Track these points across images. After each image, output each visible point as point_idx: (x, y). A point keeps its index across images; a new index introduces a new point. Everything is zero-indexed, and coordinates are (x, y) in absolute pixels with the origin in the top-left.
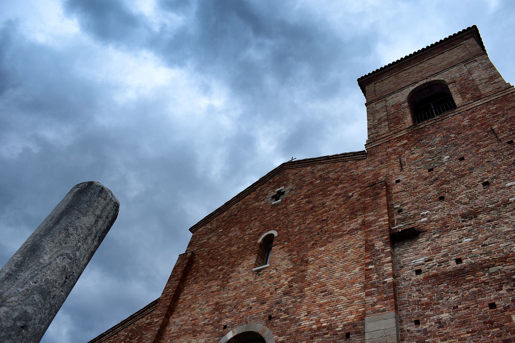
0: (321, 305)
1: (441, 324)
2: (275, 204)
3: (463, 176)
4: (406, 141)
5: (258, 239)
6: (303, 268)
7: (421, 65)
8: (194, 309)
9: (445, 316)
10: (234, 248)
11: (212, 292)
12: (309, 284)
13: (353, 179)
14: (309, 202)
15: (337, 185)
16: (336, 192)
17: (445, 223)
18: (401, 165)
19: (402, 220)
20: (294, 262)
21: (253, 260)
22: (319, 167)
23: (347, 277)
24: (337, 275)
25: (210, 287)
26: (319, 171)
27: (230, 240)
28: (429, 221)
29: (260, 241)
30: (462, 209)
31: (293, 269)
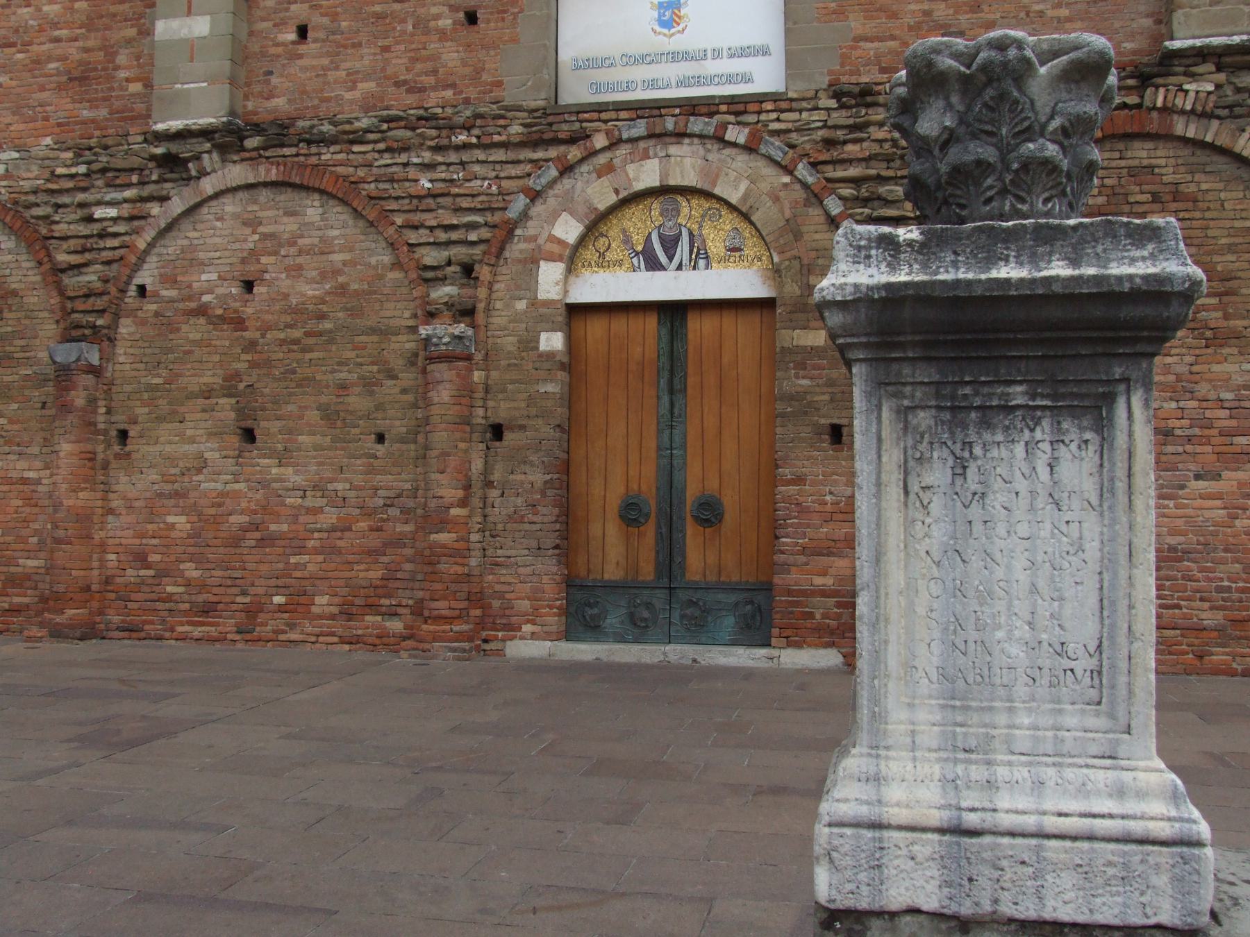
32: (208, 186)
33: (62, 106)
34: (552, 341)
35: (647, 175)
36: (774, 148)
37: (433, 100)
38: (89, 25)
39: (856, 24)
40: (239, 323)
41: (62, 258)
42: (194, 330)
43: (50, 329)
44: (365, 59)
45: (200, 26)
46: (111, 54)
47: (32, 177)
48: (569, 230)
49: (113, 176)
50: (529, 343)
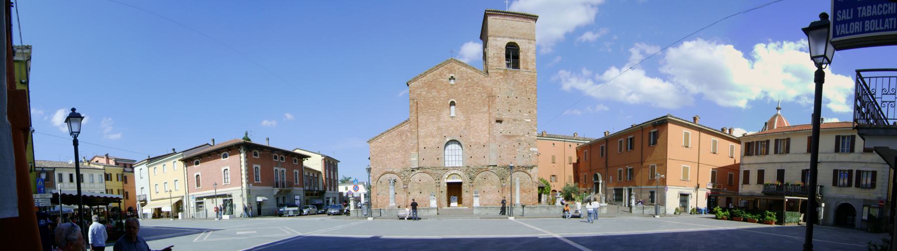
0: (477, 136)
1: (504, 148)
2: (452, 85)
3: (516, 105)
4: (502, 77)
5: (448, 102)
6: (469, 121)
7: (513, 22)
8: (428, 127)
9: (505, 146)
10: (437, 102)
11: (434, 121)
12: (472, 128)
13: (484, 87)
14: (467, 91)
15: (478, 87)
16: (478, 91)
17: (509, 120)
18: (500, 89)
19: (499, 114)
20: (465, 118)
21: (448, 112)
22: (471, 71)
23: (484, 128)
24: (480, 127)
25: (432, 119)
26: (470, 73)
27: (434, 97)
28: (505, 118)
29: (449, 103)
30: (513, 117)
31: (465, 121)
32: (416, 172)
33: (401, 165)
34: (446, 185)
35: (453, 172)
36: (462, 170)
37: (436, 166)
38: (404, 157)
39: (468, 161)
40: (419, 184)
41: (402, 178)
42: (415, 184)
43: (402, 184)
44: (429, 162)
45: (415, 159)
46: (406, 160)
47: (399, 171)
48: (447, 176)
49: (407, 171)
50: (444, 185)
